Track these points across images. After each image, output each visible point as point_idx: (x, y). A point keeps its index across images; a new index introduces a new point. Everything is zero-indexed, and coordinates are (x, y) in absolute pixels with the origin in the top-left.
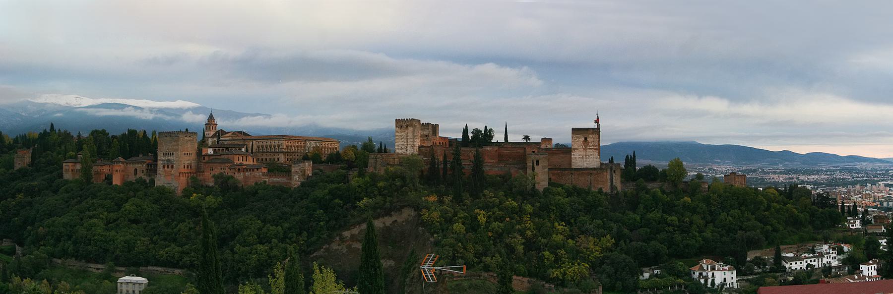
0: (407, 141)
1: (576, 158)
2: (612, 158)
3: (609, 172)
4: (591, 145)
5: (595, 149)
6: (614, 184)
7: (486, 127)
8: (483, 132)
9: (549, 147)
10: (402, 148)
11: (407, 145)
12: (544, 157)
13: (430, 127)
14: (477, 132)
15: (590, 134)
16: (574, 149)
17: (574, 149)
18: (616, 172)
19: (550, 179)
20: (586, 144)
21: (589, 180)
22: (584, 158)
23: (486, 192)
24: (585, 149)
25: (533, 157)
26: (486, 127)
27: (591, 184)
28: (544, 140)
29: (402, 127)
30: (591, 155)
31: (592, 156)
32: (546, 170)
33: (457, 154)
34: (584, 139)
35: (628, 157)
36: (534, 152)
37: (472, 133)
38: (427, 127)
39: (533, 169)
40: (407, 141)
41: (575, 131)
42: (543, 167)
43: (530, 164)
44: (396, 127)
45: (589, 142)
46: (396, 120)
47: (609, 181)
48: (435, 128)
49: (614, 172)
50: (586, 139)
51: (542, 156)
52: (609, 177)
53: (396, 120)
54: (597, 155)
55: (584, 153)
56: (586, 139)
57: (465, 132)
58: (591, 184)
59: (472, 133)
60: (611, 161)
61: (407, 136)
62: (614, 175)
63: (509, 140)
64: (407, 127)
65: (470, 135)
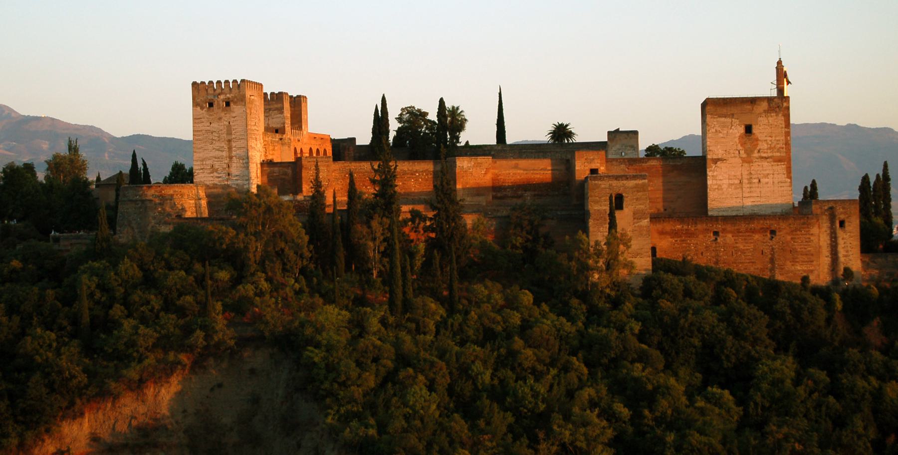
0: (230, 148)
1: (719, 188)
2: (813, 185)
3: (825, 225)
4: (763, 146)
5: (779, 160)
6: (842, 259)
7: (442, 102)
8: (433, 116)
9: (631, 155)
10: (213, 169)
11: (231, 158)
12: (637, 186)
13: (287, 105)
14: (414, 117)
15: (760, 115)
16: (715, 161)
17: (715, 161)
18: (846, 224)
19: (654, 250)
20: (748, 146)
21: (767, 251)
22: (745, 185)
23: (480, 289)
24: (748, 161)
25: (604, 184)
26: (442, 102)
27: (772, 260)
28: (614, 135)
29: (211, 105)
30: (767, 176)
31: (769, 180)
32: (645, 222)
33: (386, 182)
34: (742, 130)
35: (869, 183)
36: (594, 171)
37: (400, 119)
38: (279, 106)
39: (613, 225)
40: (230, 148)
41: (712, 107)
42: (638, 216)
43: (598, 206)
44: (196, 104)
45: (757, 140)
46: (194, 84)
47: (826, 252)
48: (298, 103)
49: (842, 224)
50: (748, 129)
51: (632, 183)
52: (824, 240)
53: (194, 84)
54: (783, 177)
55: (745, 173)
56: (748, 129)
57: (380, 121)
58: (772, 260)
59: (400, 119)
60: (811, 194)
61: (229, 133)
62: (840, 233)
63: (510, 140)
64: (228, 104)
65: (394, 126)
